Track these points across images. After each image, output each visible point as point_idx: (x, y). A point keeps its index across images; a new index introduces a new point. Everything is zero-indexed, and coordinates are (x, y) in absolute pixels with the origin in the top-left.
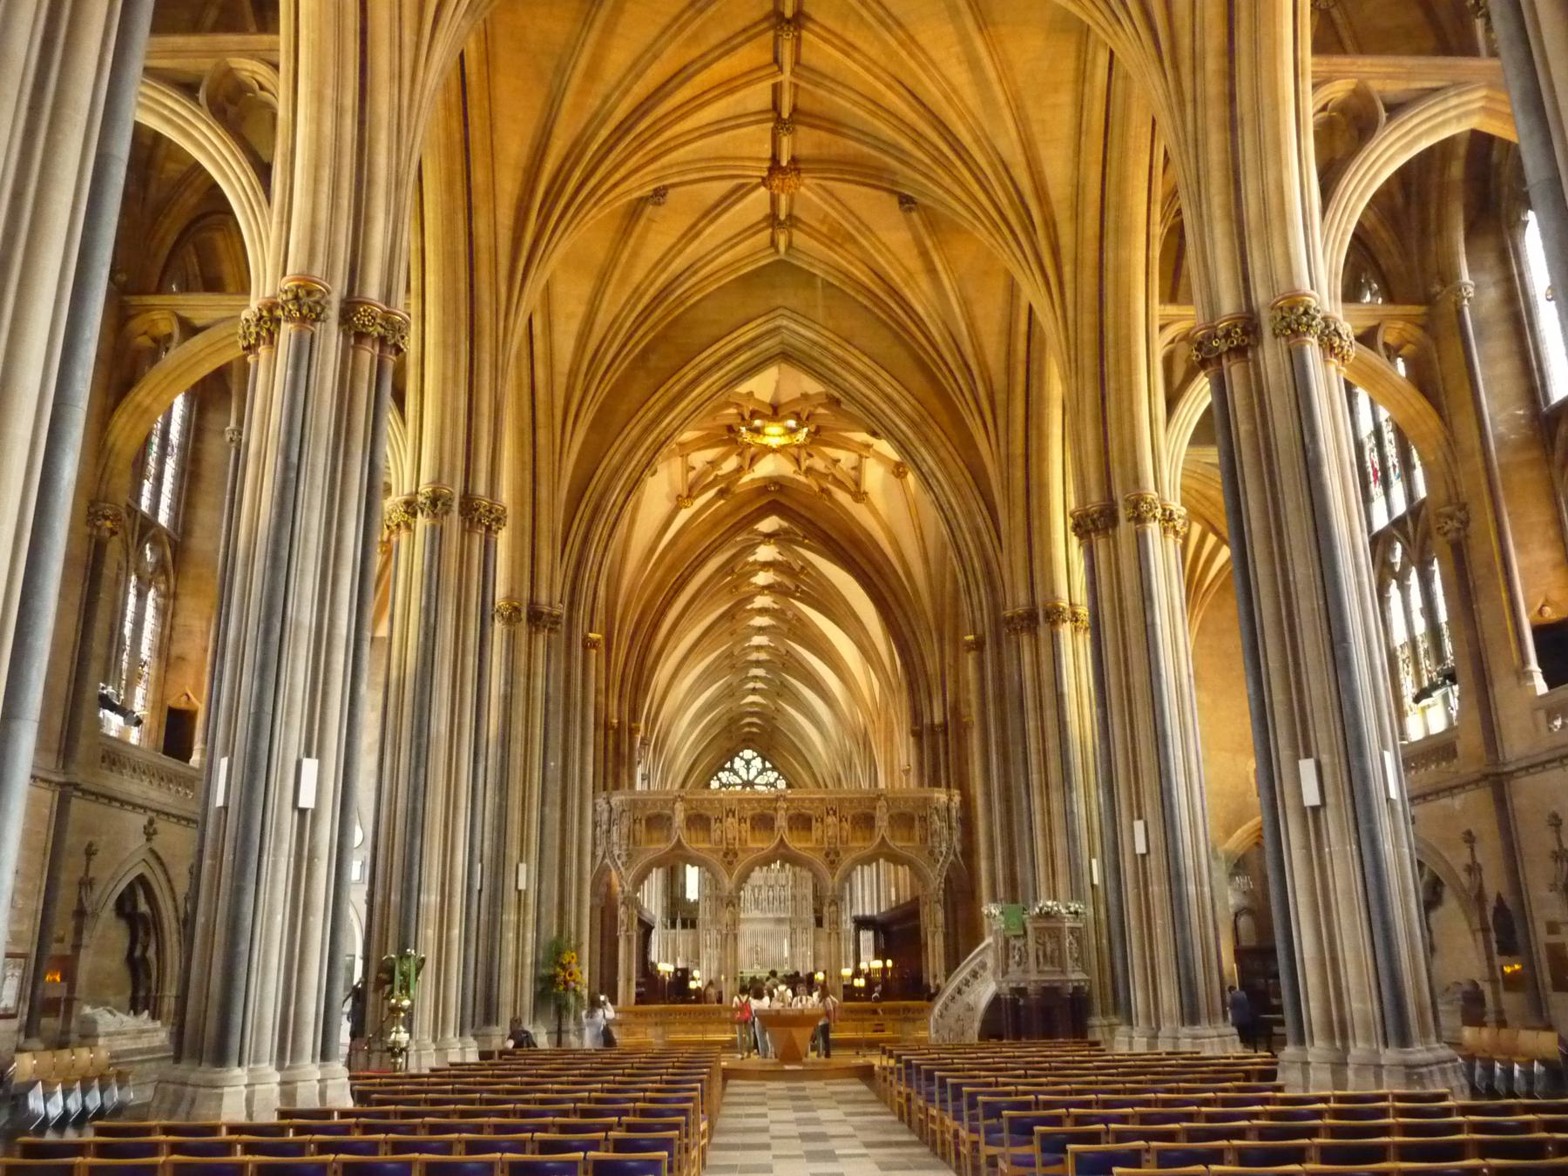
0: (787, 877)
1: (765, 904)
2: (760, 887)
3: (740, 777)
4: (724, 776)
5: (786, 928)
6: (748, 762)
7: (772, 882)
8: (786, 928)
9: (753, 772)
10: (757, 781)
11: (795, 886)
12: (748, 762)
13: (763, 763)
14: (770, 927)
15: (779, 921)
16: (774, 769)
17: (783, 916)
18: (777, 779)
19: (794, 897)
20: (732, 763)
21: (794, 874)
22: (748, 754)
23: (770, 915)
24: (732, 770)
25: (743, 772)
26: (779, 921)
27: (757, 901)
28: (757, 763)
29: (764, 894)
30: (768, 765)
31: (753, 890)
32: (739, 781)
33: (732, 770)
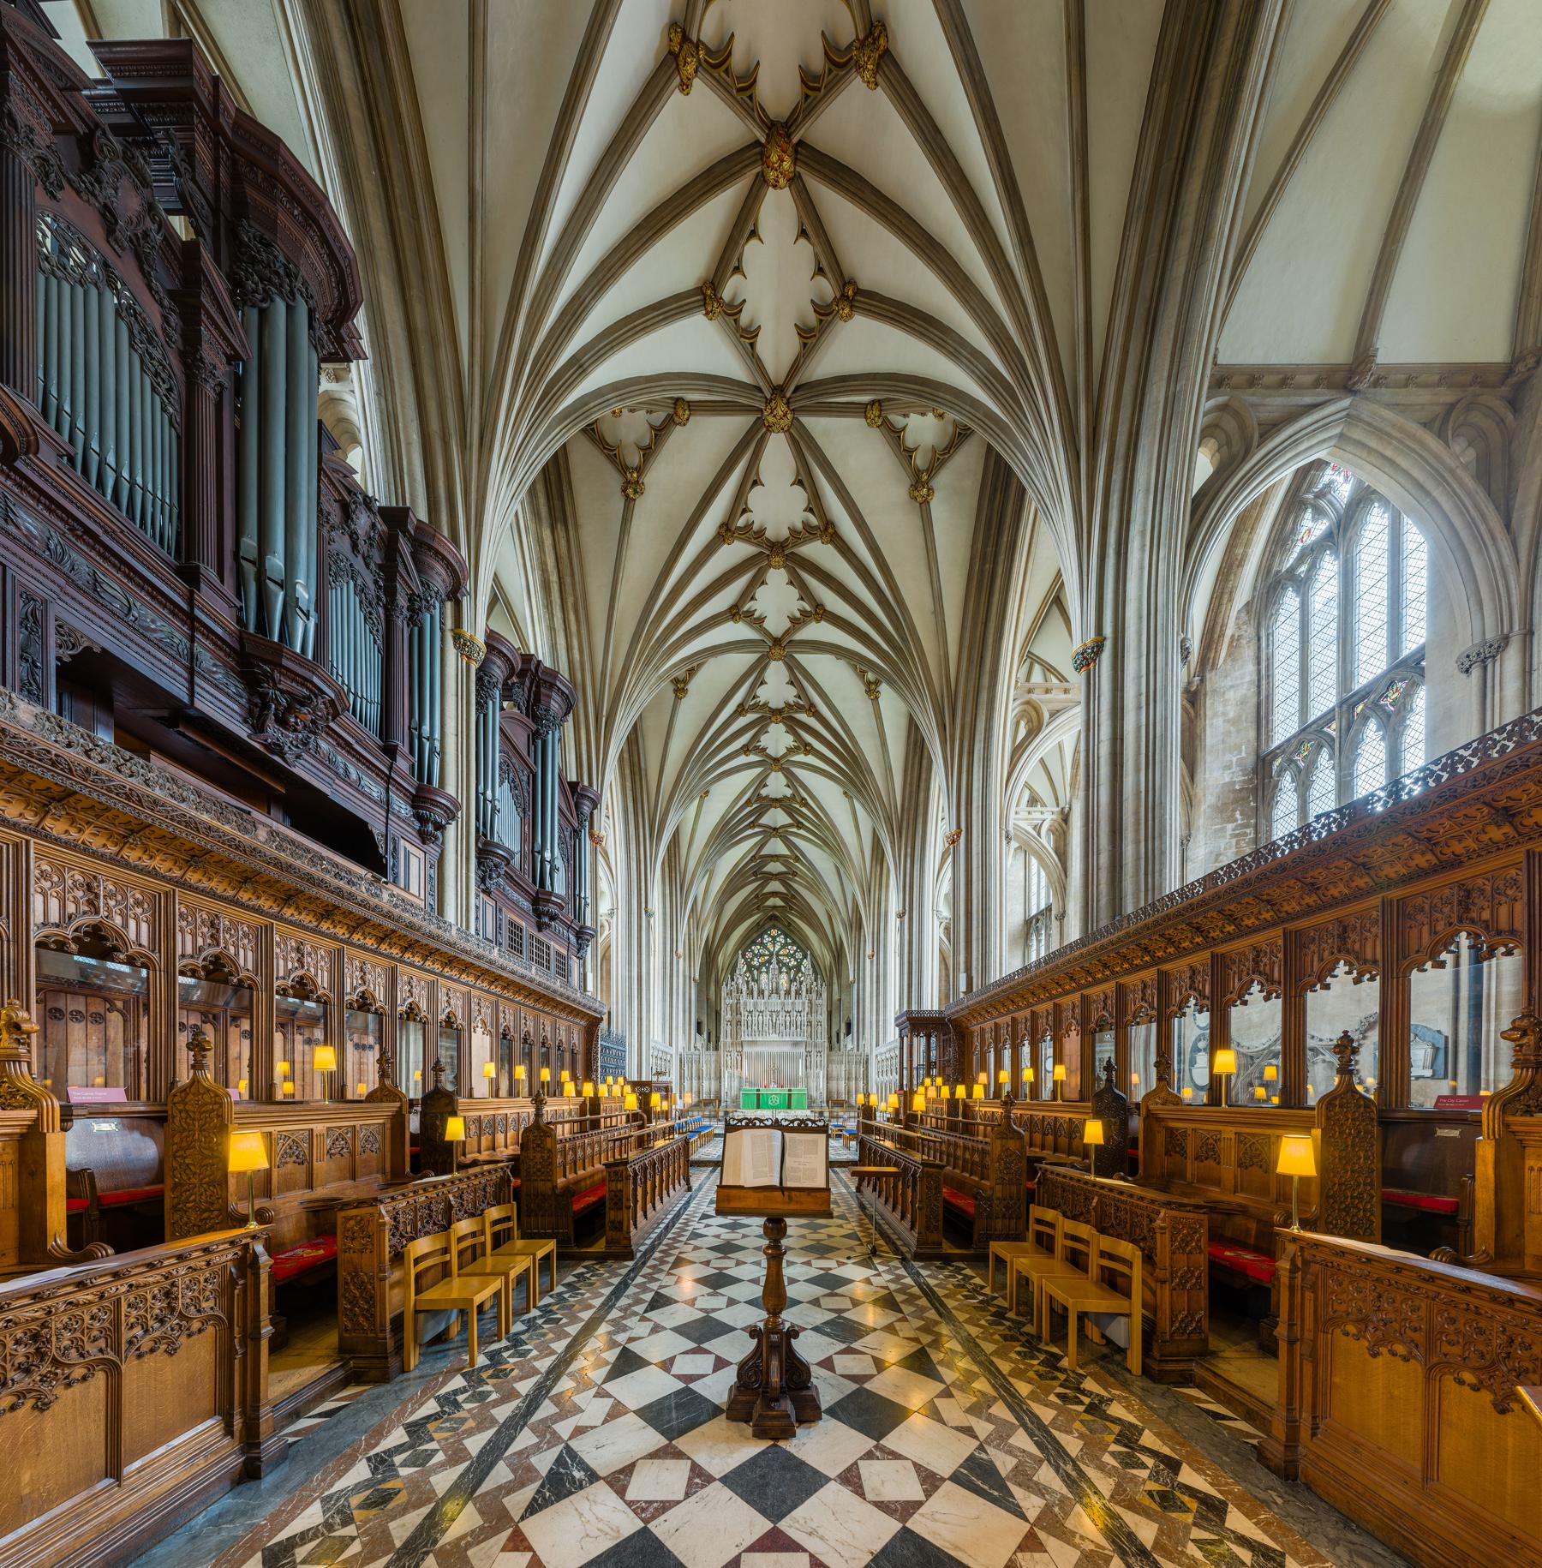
0: (803, 1003)
1: (782, 1028)
4: (756, 949)
6: (774, 938)
7: (789, 1008)
9: (778, 947)
12: (774, 938)
14: (787, 1049)
15: (796, 1044)
16: (794, 943)
17: (799, 1039)
19: (810, 1023)
20: (763, 939)
21: (811, 1002)
22: (774, 932)
23: (788, 1039)
24: (762, 944)
25: (770, 946)
26: (796, 1044)
27: (774, 1026)
28: (781, 939)
33: (762, 944)
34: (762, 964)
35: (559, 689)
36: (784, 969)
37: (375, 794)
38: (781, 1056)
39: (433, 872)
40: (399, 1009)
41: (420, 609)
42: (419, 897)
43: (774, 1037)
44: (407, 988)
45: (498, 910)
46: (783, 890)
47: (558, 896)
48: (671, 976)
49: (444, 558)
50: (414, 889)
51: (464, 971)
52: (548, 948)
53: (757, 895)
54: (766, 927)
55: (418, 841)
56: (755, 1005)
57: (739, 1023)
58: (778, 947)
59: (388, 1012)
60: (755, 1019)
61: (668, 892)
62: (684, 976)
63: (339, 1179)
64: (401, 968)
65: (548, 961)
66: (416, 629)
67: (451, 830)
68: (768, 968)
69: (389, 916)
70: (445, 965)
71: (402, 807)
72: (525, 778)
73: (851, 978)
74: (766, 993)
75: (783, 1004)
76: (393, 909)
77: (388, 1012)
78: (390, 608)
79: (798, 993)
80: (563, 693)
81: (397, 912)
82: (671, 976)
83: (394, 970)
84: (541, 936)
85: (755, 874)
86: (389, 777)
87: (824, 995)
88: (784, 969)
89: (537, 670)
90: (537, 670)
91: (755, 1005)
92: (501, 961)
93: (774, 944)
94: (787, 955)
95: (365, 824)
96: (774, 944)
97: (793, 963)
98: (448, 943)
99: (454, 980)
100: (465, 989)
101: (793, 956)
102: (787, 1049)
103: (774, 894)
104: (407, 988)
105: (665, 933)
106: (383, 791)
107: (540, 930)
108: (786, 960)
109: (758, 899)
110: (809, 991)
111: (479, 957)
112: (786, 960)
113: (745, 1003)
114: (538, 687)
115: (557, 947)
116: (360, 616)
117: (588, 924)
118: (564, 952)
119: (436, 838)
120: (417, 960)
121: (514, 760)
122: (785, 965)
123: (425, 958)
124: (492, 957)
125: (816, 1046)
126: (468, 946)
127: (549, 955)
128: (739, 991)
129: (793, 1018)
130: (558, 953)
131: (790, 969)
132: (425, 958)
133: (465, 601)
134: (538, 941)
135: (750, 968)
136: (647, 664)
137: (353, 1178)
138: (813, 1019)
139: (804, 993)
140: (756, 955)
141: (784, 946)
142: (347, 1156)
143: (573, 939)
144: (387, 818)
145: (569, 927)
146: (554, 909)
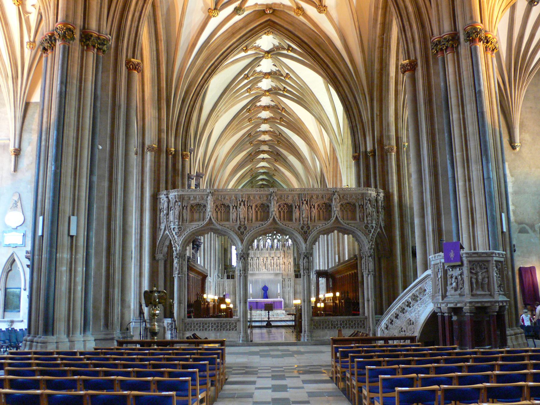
0: (280, 253)
2: (267, 258)
5: (280, 278)
7: (273, 256)
17: (278, 272)
23: (273, 272)
27: (265, 265)
29: (269, 261)
56: (255, 254)
60: (255, 262)
75: (270, 254)
102: (272, 277)
103: (265, 132)
109: (250, 137)
129: (275, 261)
138: (286, 261)
139: (281, 247)
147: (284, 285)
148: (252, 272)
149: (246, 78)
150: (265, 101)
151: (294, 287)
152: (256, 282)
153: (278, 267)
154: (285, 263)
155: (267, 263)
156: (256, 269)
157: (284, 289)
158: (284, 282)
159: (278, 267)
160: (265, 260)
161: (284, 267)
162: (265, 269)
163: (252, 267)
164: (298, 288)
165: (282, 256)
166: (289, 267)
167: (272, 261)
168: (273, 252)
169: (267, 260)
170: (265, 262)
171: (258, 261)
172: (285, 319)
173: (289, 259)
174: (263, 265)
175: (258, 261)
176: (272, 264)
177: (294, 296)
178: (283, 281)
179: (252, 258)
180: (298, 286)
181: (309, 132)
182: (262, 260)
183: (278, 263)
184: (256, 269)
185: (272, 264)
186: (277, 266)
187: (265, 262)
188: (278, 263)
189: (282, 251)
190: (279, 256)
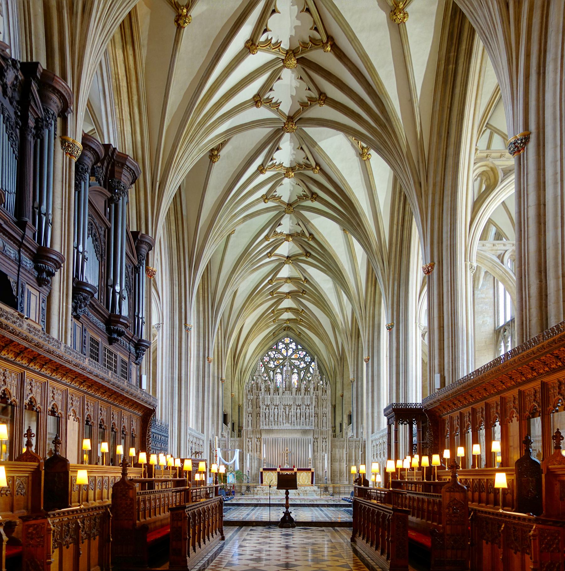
0: (311, 398)
1: (294, 419)
2: (290, 406)
3: (282, 355)
5: (310, 437)
6: (287, 345)
8: (310, 437)
9: (290, 352)
10: (293, 357)
11: (317, 406)
12: (287, 345)
13: (296, 346)
14: (298, 436)
15: (305, 432)
16: (303, 349)
17: (308, 428)
18: (305, 356)
19: (316, 414)
21: (317, 397)
22: (287, 340)
23: (298, 428)
25: (284, 351)
26: (305, 432)
28: (293, 346)
30: (299, 347)
31: (285, 409)
32: (281, 357)
34: (276, 366)
35: (128, 167)
36: (295, 371)
37: (12, 255)
38: (293, 441)
39: (44, 305)
40: (25, 401)
41: (42, 127)
42: (35, 322)
43: (287, 426)
44: (29, 387)
45: (84, 330)
46: (294, 306)
47: (124, 318)
48: (204, 377)
49: (59, 92)
50: (33, 317)
51: (64, 375)
52: (116, 356)
53: (273, 312)
54: (281, 335)
55: (36, 285)
56: (272, 400)
57: (258, 414)
58: (290, 352)
59: (18, 404)
60: (272, 411)
61: (201, 309)
62: (214, 377)
63: (5, 511)
64: (27, 373)
65: (116, 367)
66: (39, 140)
67: (56, 278)
68: (282, 370)
69: (26, 339)
70: (53, 371)
71: (27, 262)
72: (102, 233)
73: (351, 377)
74: (281, 391)
76: (28, 334)
77: (18, 404)
78: (24, 129)
79: (306, 390)
80: (131, 169)
81: (31, 336)
82: (204, 377)
83: (22, 375)
84: (110, 348)
85: (272, 293)
86: (22, 243)
87: (329, 392)
88: (295, 371)
89: (113, 154)
90: (113, 154)
91: (272, 400)
92: (90, 367)
93: (287, 350)
94: (297, 359)
95: (7, 275)
96: (287, 350)
97: (303, 365)
98: (59, 356)
99: (58, 382)
100: (64, 387)
101: (302, 359)
102: (298, 436)
104: (29, 387)
105: (199, 342)
106: (17, 253)
107: (110, 344)
108: (297, 363)
110: (316, 388)
111: (76, 365)
112: (297, 363)
113: (264, 399)
114: (113, 166)
115: (122, 356)
116: (6, 136)
117: (144, 338)
118: (126, 360)
119: (48, 282)
120: (36, 368)
121: (96, 221)
122: (297, 367)
123: (42, 367)
124: (84, 365)
125: (322, 433)
126: (70, 358)
127: (116, 362)
128: (258, 388)
130: (123, 361)
131: (299, 370)
132: (42, 367)
133: (70, 117)
134: (109, 352)
135: (267, 369)
136: (191, 142)
137: (12, 511)
139: (312, 390)
140: (271, 359)
141: (294, 352)
142: (9, 495)
143: (133, 349)
144: (19, 271)
145: (130, 340)
146: (122, 328)
147: (316, 448)
148: (267, 428)
149: (270, 284)
150: (287, 303)
151: (332, 451)
152: (275, 442)
153: (307, 420)
154: (317, 414)
155: (290, 414)
156: (273, 423)
157: (316, 454)
158: (316, 443)
159: (307, 420)
160: (287, 409)
161: (316, 421)
162: (287, 424)
163: (267, 420)
164: (337, 452)
165: (314, 403)
166: (324, 421)
167: (299, 411)
168: (300, 397)
169: (290, 409)
170: (287, 413)
171: (276, 410)
172: (318, 503)
173: (324, 409)
174: (284, 417)
175: (276, 410)
176: (298, 415)
177: (331, 464)
178: (314, 442)
179: (267, 406)
180: (337, 450)
181: (386, 94)
182: (282, 410)
183: (307, 414)
184: (273, 423)
185: (298, 415)
186: (306, 419)
187: (287, 413)
188: (307, 414)
189: (314, 397)
190: (309, 403)
